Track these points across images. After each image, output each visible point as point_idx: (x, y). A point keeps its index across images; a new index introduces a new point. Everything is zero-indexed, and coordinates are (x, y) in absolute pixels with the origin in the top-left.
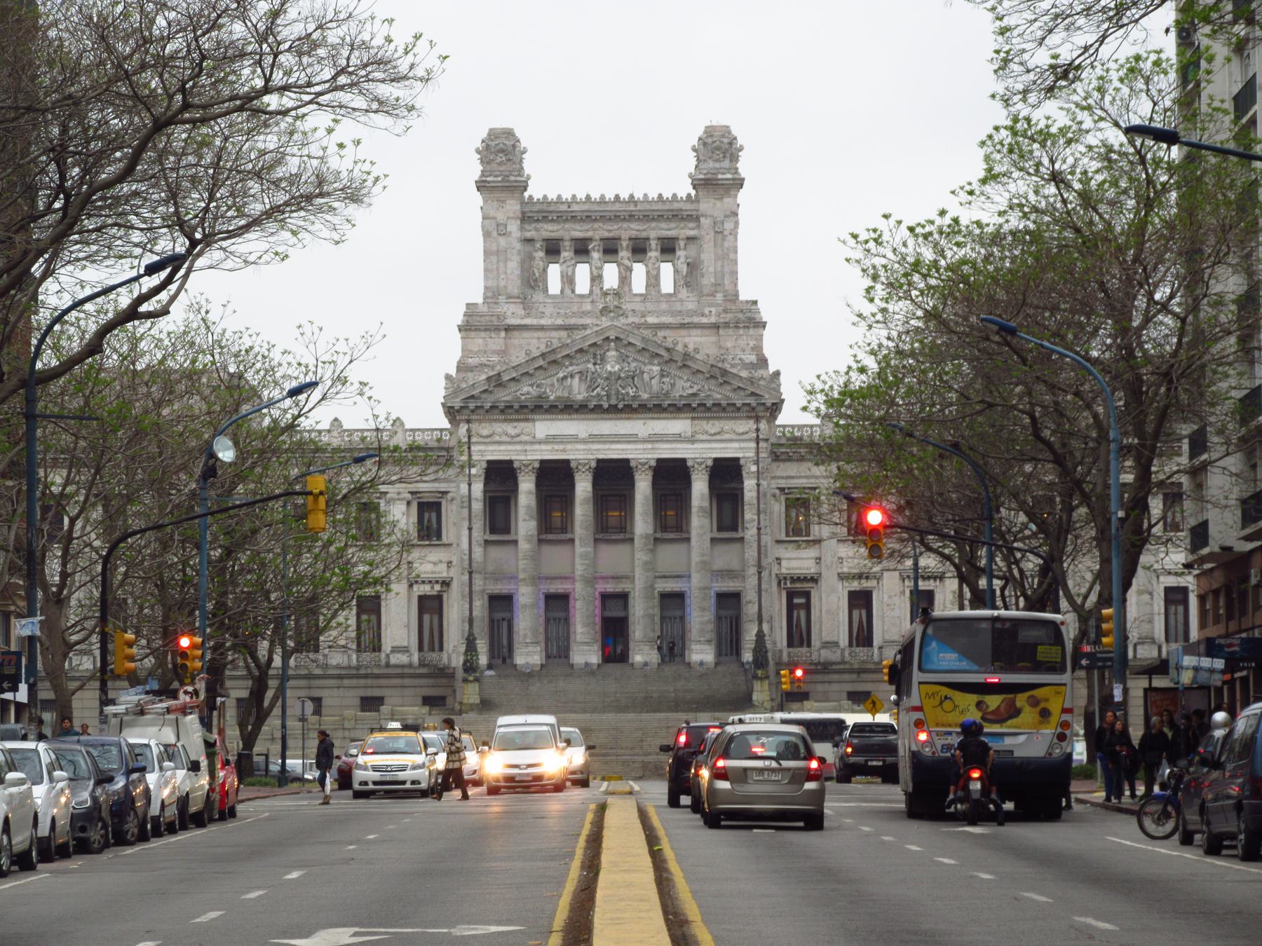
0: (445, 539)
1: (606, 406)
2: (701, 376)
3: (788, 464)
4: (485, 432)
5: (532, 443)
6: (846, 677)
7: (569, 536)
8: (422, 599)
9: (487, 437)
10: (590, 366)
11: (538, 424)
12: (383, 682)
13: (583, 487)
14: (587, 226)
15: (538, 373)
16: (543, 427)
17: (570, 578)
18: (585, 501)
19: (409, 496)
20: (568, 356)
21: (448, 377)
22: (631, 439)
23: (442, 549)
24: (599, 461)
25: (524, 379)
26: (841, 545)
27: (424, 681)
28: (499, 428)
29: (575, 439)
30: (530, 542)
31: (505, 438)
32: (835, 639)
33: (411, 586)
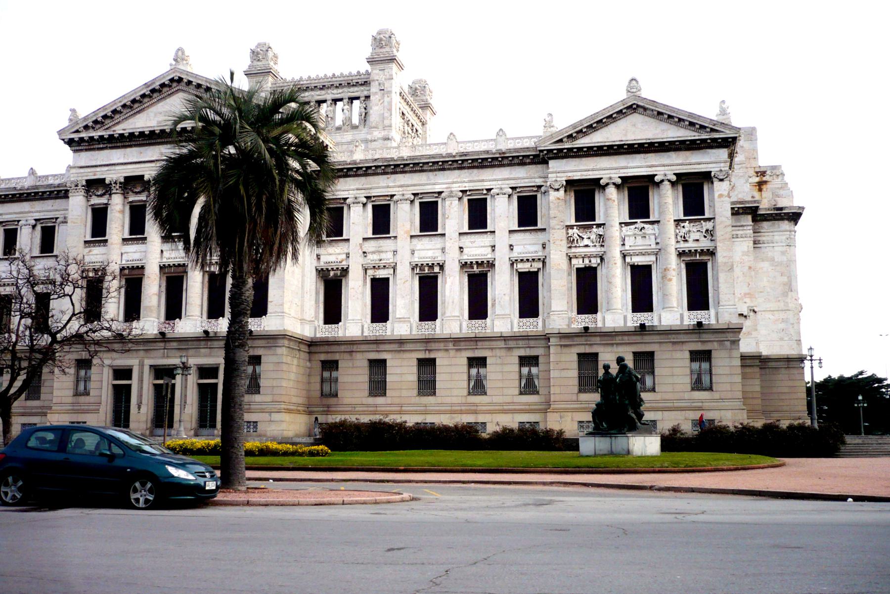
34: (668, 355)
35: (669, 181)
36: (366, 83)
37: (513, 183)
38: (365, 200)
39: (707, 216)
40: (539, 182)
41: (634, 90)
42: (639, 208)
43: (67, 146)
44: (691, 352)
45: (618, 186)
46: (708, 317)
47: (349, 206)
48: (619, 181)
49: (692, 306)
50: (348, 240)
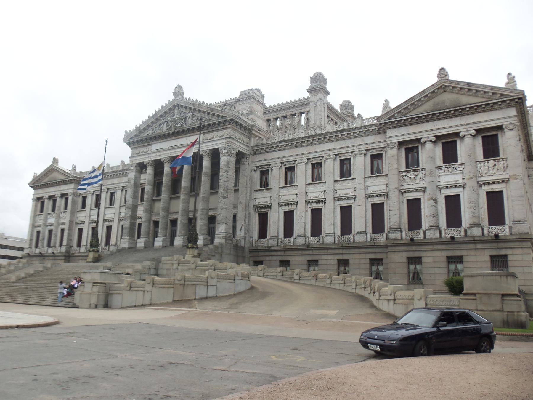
1: (171, 132)
3: (260, 155)
4: (137, 152)
5: (150, 153)
6: (279, 253)
7: (178, 195)
13: (167, 169)
15: (154, 125)
16: (155, 147)
17: (177, 212)
18: (167, 175)
20: (161, 116)
21: (126, 132)
25: (150, 128)
26: (281, 189)
29: (163, 150)
30: (146, 194)
32: (276, 235)
34: (473, 258)
35: (471, 135)
36: (308, 104)
37: (367, 147)
38: (280, 164)
39: (502, 156)
40: (382, 145)
41: (442, 76)
42: (450, 155)
43: (128, 147)
44: (491, 256)
45: (434, 142)
46: (504, 231)
47: (272, 169)
48: (434, 139)
49: (492, 223)
50: (271, 189)
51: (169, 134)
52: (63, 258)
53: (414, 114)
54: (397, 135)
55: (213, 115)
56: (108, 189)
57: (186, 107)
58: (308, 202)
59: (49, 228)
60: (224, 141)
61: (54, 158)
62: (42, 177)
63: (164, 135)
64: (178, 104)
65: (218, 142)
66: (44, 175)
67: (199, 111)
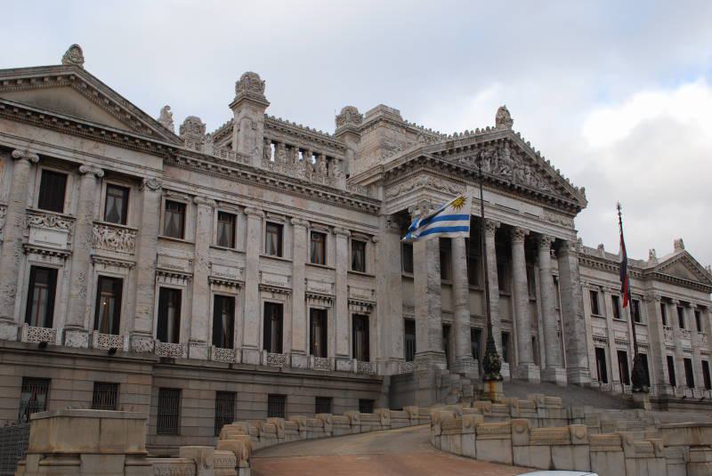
0: (369, 271)
2: (547, 181)
8: (355, 317)
9: (440, 188)
10: (496, 154)
11: (468, 187)
12: (332, 384)
14: (293, 139)
19: (349, 232)
20: (486, 144)
22: (515, 212)
23: (368, 279)
24: (502, 224)
27: (361, 386)
28: (446, 184)
31: (449, 192)
33: (349, 303)
40: (641, 292)
51: (505, 184)
52: (147, 369)
53: (668, 273)
54: (660, 289)
55: (562, 189)
56: (266, 212)
57: (524, 154)
58: (595, 339)
59: (35, 259)
60: (570, 233)
61: (76, 48)
62: (15, 81)
63: (497, 181)
64: (510, 142)
65: (564, 231)
66: (28, 80)
67: (543, 172)
